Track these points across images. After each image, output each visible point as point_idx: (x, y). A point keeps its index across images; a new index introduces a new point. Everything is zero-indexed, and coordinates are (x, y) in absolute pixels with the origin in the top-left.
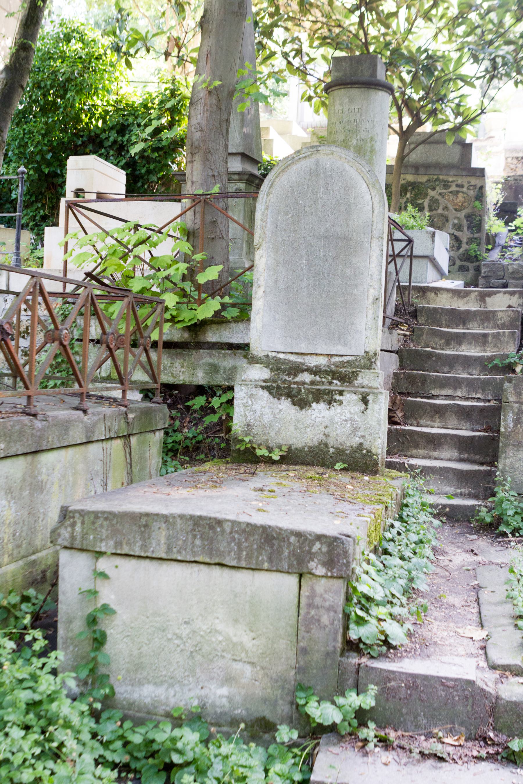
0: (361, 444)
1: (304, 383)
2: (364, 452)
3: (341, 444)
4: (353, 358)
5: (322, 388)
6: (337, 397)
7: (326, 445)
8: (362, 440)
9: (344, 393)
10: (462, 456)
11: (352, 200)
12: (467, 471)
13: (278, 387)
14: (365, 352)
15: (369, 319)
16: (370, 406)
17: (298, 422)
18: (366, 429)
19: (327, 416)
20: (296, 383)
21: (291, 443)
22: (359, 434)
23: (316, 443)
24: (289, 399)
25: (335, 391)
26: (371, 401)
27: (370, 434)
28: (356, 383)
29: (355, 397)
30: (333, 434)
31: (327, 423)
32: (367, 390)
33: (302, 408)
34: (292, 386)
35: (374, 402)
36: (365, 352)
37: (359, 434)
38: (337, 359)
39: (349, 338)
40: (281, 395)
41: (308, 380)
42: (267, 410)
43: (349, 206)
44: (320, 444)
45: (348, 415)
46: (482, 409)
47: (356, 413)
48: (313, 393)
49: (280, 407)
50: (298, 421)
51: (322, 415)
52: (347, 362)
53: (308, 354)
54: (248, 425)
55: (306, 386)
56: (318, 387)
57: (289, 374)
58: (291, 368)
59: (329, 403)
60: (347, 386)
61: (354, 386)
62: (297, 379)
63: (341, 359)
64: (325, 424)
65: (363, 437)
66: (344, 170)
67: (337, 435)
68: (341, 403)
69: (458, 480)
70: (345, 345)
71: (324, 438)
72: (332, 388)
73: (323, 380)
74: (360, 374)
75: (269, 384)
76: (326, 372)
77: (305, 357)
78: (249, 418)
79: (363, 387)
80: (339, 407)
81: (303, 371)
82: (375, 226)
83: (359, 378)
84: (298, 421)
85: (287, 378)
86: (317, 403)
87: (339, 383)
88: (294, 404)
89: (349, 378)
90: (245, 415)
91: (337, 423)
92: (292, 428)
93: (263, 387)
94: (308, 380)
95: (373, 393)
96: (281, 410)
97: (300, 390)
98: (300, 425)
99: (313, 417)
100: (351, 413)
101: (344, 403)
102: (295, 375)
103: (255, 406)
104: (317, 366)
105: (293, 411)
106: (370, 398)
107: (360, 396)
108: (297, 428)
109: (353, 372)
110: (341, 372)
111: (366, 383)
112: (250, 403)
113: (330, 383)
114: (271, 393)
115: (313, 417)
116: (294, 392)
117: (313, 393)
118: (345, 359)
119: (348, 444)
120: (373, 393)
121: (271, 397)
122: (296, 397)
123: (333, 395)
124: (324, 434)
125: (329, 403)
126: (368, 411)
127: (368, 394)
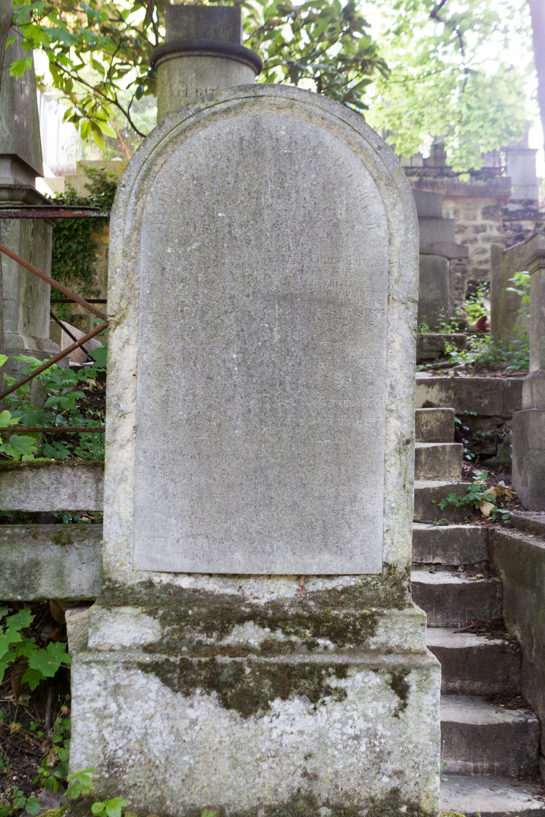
0: (395, 792)
1: (246, 649)
2: (404, 809)
3: (347, 796)
4: (359, 581)
5: (297, 659)
6: (333, 682)
7: (311, 800)
8: (396, 783)
9: (349, 672)
10: (451, 685)
11: (342, 213)
12: (484, 728)
13: (185, 665)
14: (386, 564)
15: (390, 488)
16: (412, 698)
17: (238, 749)
18: (405, 754)
19: (308, 730)
20: (227, 650)
21: (223, 801)
22: (389, 767)
23: (286, 797)
24: (214, 694)
25: (326, 667)
26: (413, 688)
27: (416, 767)
28: (373, 642)
29: (375, 680)
30: (326, 773)
31: (310, 745)
32: (402, 660)
33: (246, 714)
34: (221, 659)
35: (421, 688)
36: (386, 564)
37: (389, 767)
38: (321, 585)
39: (348, 535)
40: (194, 684)
41: (254, 643)
42: (158, 723)
43: (336, 226)
44: (295, 798)
45: (361, 724)
46: (460, 590)
47: (379, 716)
48: (272, 676)
49: (191, 713)
50: (237, 745)
51: (298, 726)
52: (345, 590)
53: (249, 576)
54: (111, 765)
55: (253, 657)
56: (281, 659)
57: (208, 629)
58: (213, 614)
59: (314, 697)
60: (352, 652)
61: (367, 651)
62: (229, 640)
63: (330, 585)
64: (305, 750)
65: (399, 774)
66: (320, 144)
67: (336, 773)
68: (342, 694)
69: (469, 744)
70: (339, 551)
71: (304, 783)
72: (317, 658)
73: (294, 638)
74: (381, 622)
75: (160, 657)
76: (299, 620)
77: (243, 582)
78: (112, 747)
79: (389, 652)
80: (338, 707)
81: (242, 620)
82: (395, 275)
83: (380, 631)
84: (237, 745)
85: (202, 637)
86: (284, 697)
87: (332, 646)
88: (227, 705)
89: (356, 632)
90: (103, 739)
91: (334, 745)
92: (224, 765)
93: (145, 668)
94: (254, 643)
95: (419, 668)
96: (194, 722)
97: (239, 669)
98: (243, 756)
99: (274, 735)
100: (366, 718)
101: (351, 696)
102: (224, 631)
103: (126, 716)
104: (275, 605)
105: (225, 722)
106: (411, 679)
107: (388, 677)
108: (235, 764)
109: (364, 617)
110: (335, 619)
111: (395, 640)
112: (113, 707)
113: (311, 646)
114: (166, 682)
115: (274, 735)
116: (226, 675)
117: (272, 676)
118: (339, 584)
119: (364, 795)
120: (419, 668)
121: (167, 691)
122: (231, 686)
123: (321, 678)
124: (305, 774)
125: (314, 697)
126: (409, 711)
127: (406, 671)
